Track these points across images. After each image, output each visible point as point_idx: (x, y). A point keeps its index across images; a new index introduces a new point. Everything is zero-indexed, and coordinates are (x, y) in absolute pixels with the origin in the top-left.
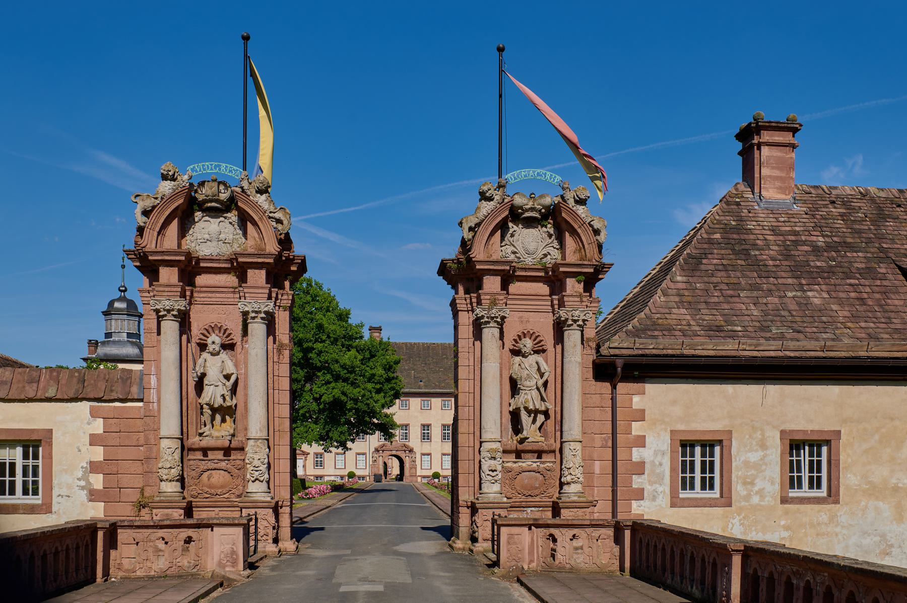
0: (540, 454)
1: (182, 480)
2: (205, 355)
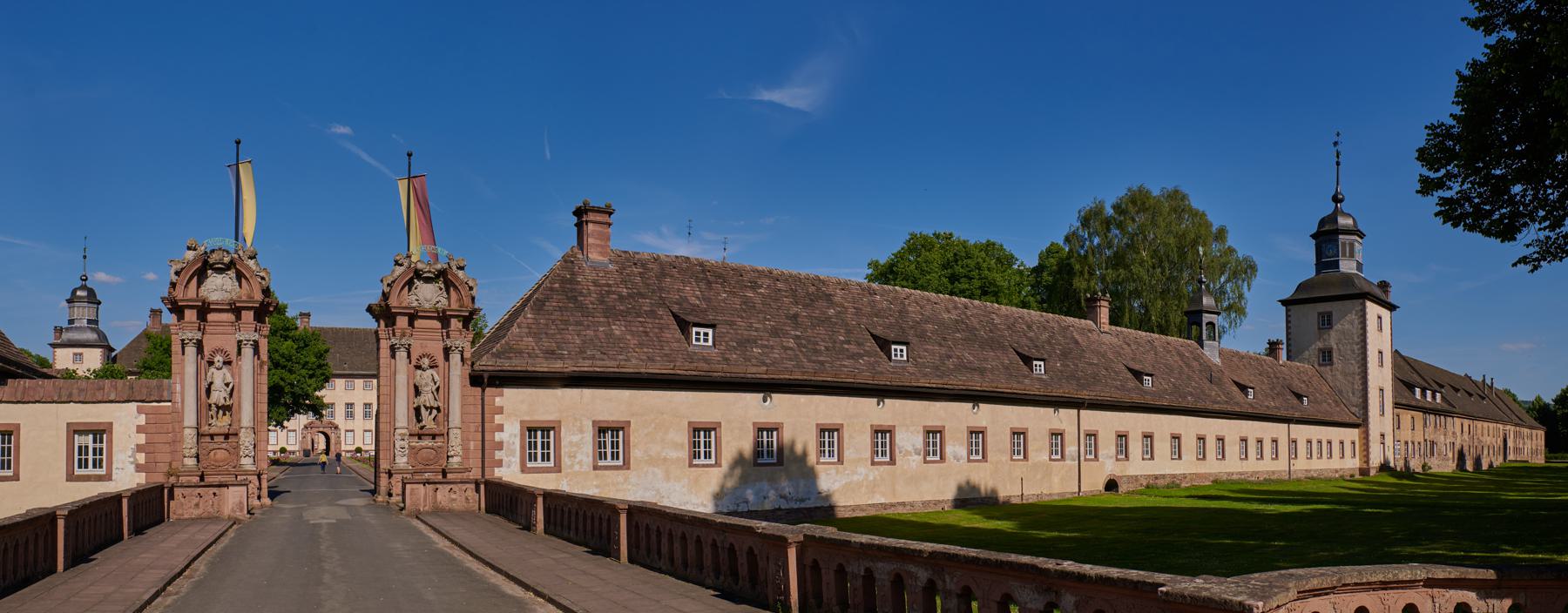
0: (434, 436)
1: (197, 457)
2: (212, 370)
